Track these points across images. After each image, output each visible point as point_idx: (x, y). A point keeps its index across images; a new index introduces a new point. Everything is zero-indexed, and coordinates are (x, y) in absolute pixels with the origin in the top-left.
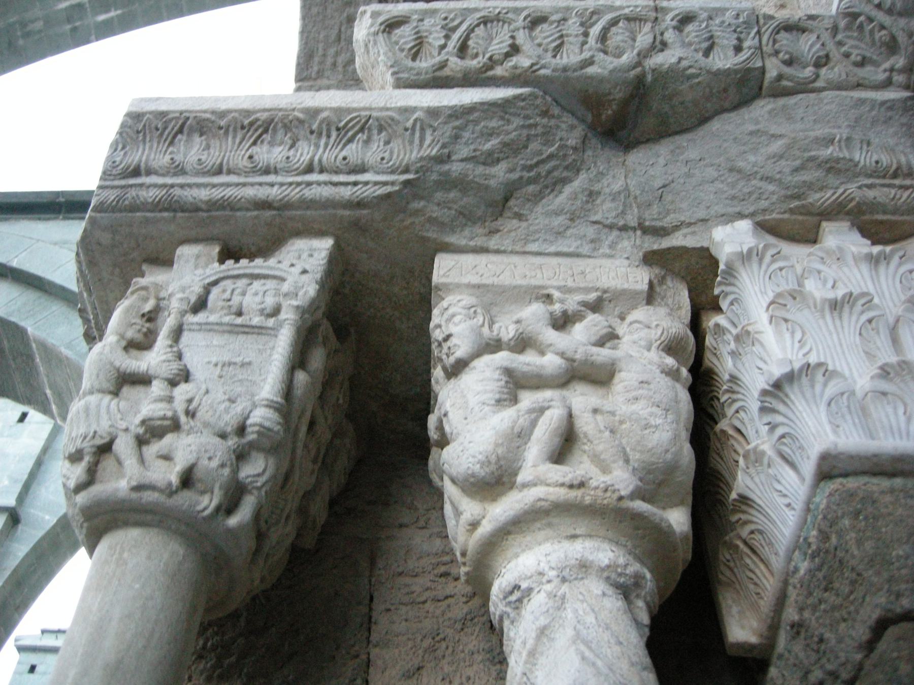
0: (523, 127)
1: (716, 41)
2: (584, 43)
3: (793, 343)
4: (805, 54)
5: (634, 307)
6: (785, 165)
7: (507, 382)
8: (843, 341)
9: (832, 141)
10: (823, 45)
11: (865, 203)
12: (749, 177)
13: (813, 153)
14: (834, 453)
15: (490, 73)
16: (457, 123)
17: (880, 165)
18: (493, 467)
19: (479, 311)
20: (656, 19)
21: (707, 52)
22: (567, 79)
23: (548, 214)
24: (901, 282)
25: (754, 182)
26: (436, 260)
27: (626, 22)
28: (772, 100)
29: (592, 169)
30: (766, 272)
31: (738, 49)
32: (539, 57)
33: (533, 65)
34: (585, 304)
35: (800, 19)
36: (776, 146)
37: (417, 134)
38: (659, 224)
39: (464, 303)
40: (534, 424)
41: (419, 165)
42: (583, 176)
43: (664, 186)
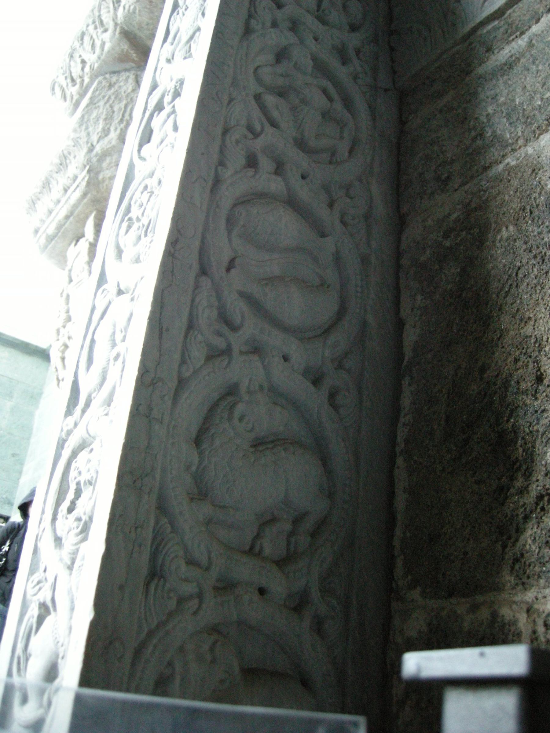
0: (106, 103)
22: (103, 60)
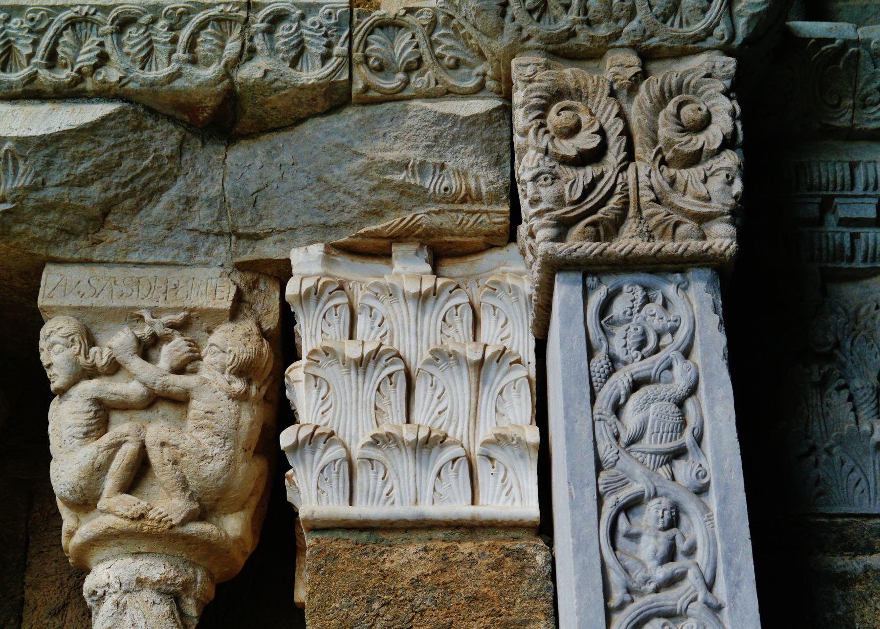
0: (115, 146)
1: (307, 45)
2: (174, 51)
3: (317, 399)
4: (396, 59)
5: (219, 323)
6: (365, 184)
7: (96, 412)
8: (360, 398)
9: (406, 166)
10: (417, 46)
11: (431, 228)
12: (334, 189)
13: (388, 177)
14: (310, 519)
15: (81, 86)
16: (47, 152)
17: (448, 192)
18: (79, 495)
19: (76, 339)
20: (247, 19)
21: (294, 64)
22: (155, 92)
23: (146, 226)
24: (444, 320)
25: (338, 194)
26: (44, 276)
27: (215, 23)
28: (360, 108)
29: (190, 173)
30: (321, 310)
31: (325, 58)
32: (127, 70)
33: (121, 79)
34: (173, 326)
35: (396, 15)
36: (357, 164)
37: (10, 164)
38: (252, 231)
39: (62, 331)
40: (111, 458)
41: (14, 195)
42: (180, 182)
43: (258, 191)
